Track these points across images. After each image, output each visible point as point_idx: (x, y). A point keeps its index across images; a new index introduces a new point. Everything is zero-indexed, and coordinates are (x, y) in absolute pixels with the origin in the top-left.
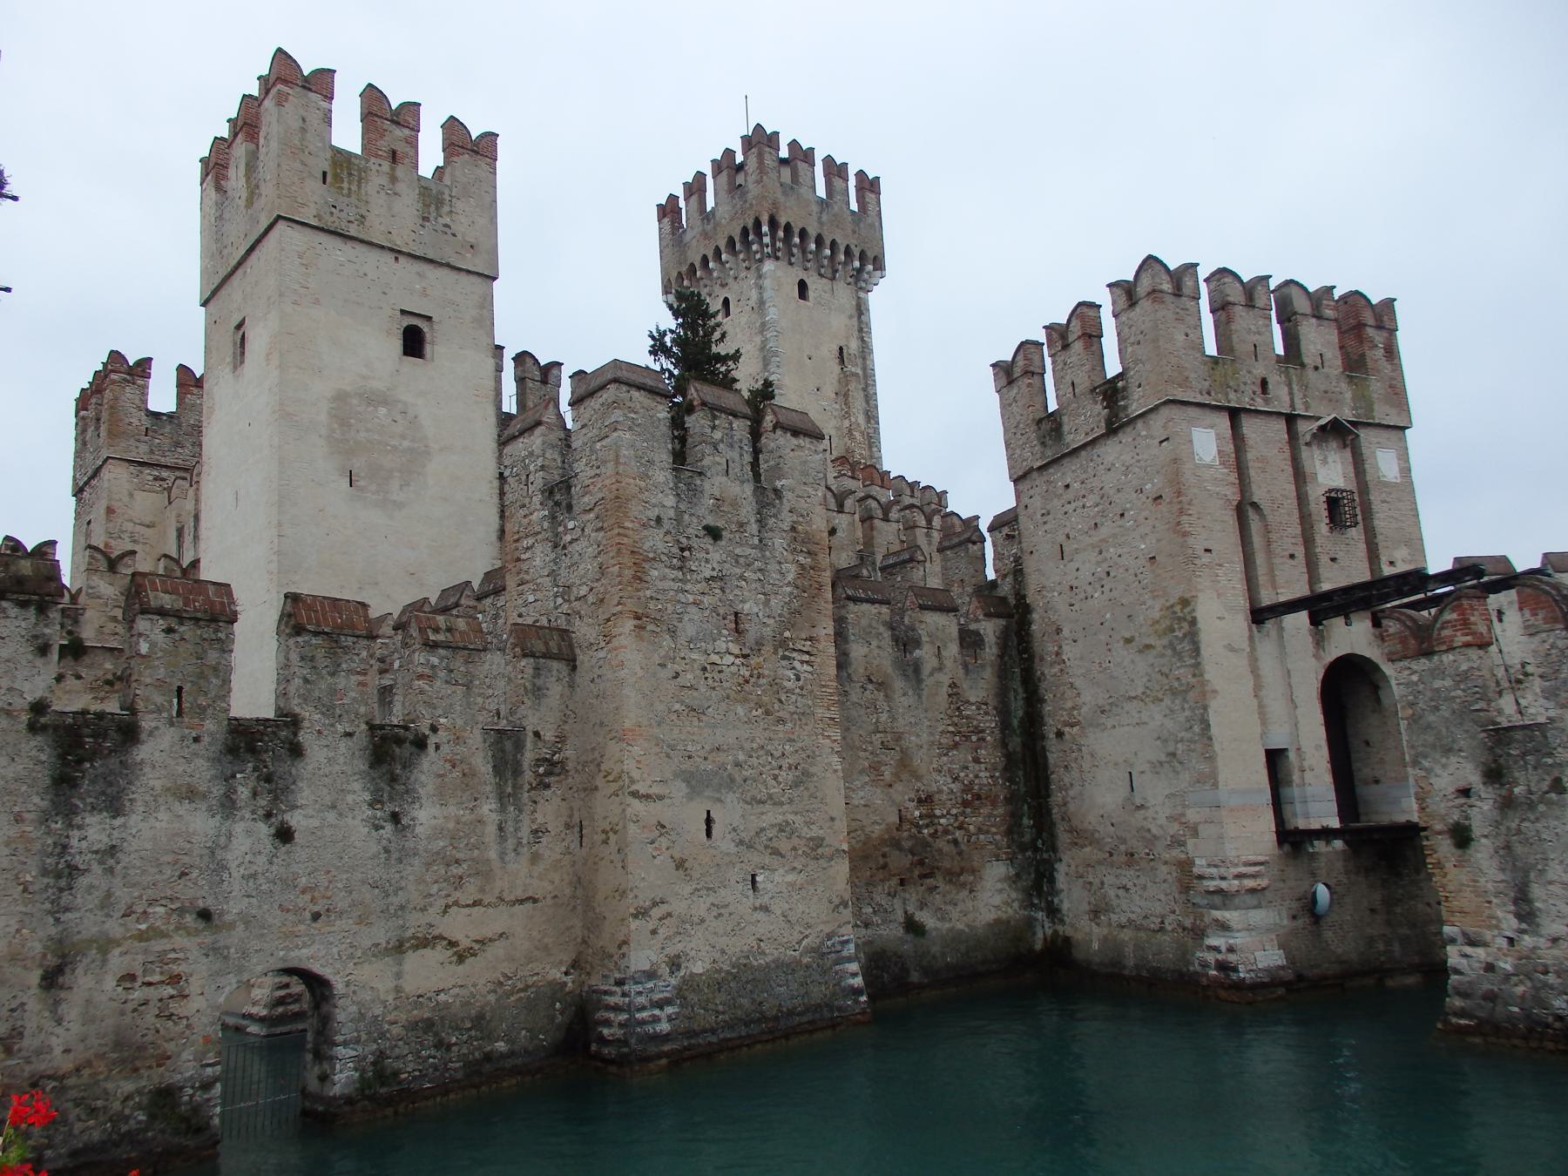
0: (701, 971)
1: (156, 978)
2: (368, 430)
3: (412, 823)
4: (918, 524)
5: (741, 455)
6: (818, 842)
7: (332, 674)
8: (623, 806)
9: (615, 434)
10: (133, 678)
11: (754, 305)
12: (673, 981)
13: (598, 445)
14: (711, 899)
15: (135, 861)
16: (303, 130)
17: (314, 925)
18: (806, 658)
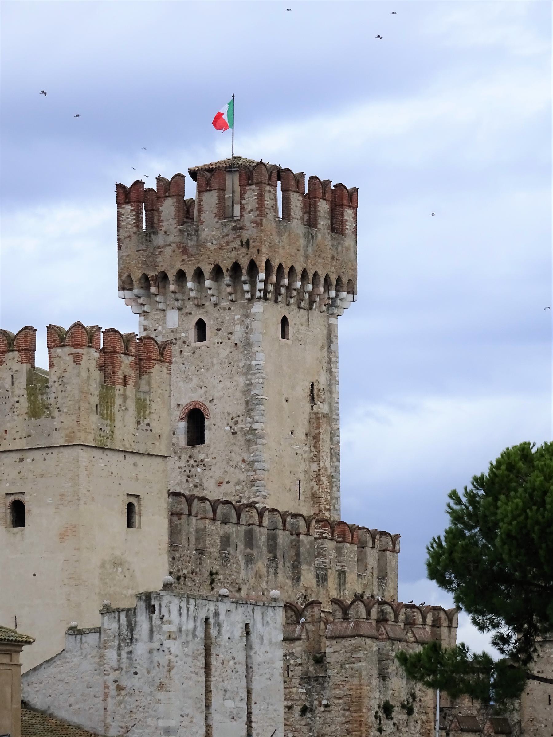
4: (417, 622)
13: (347, 666)
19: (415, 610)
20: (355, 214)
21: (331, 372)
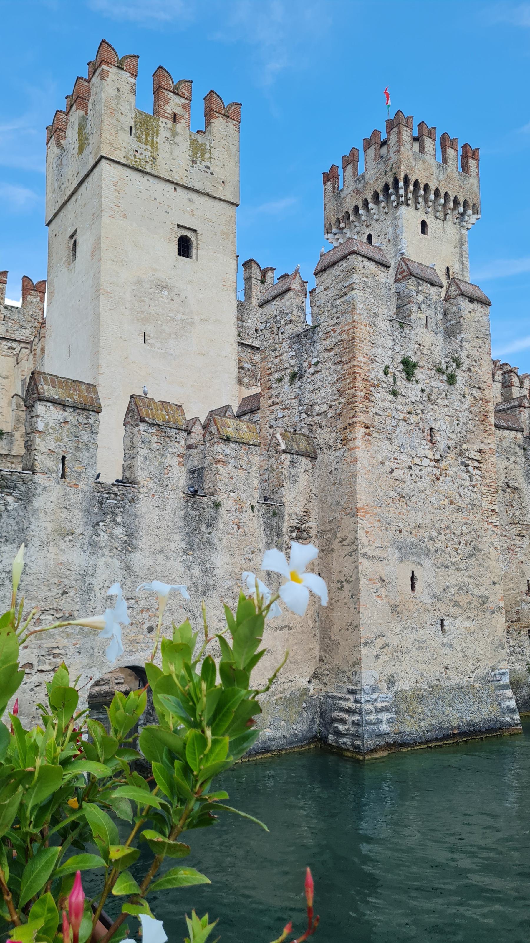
0: (408, 688)
1: (46, 667)
2: (156, 306)
3: (212, 566)
4: (514, 384)
5: (436, 314)
6: (484, 599)
7: (162, 456)
8: (355, 564)
9: (353, 292)
10: (33, 448)
11: (390, 238)
12: (390, 695)
13: (338, 302)
14: (414, 636)
15: (33, 581)
16: (118, 97)
17: (149, 635)
18: (476, 464)
19: (512, 374)
20: (478, 164)
21: (463, 263)
